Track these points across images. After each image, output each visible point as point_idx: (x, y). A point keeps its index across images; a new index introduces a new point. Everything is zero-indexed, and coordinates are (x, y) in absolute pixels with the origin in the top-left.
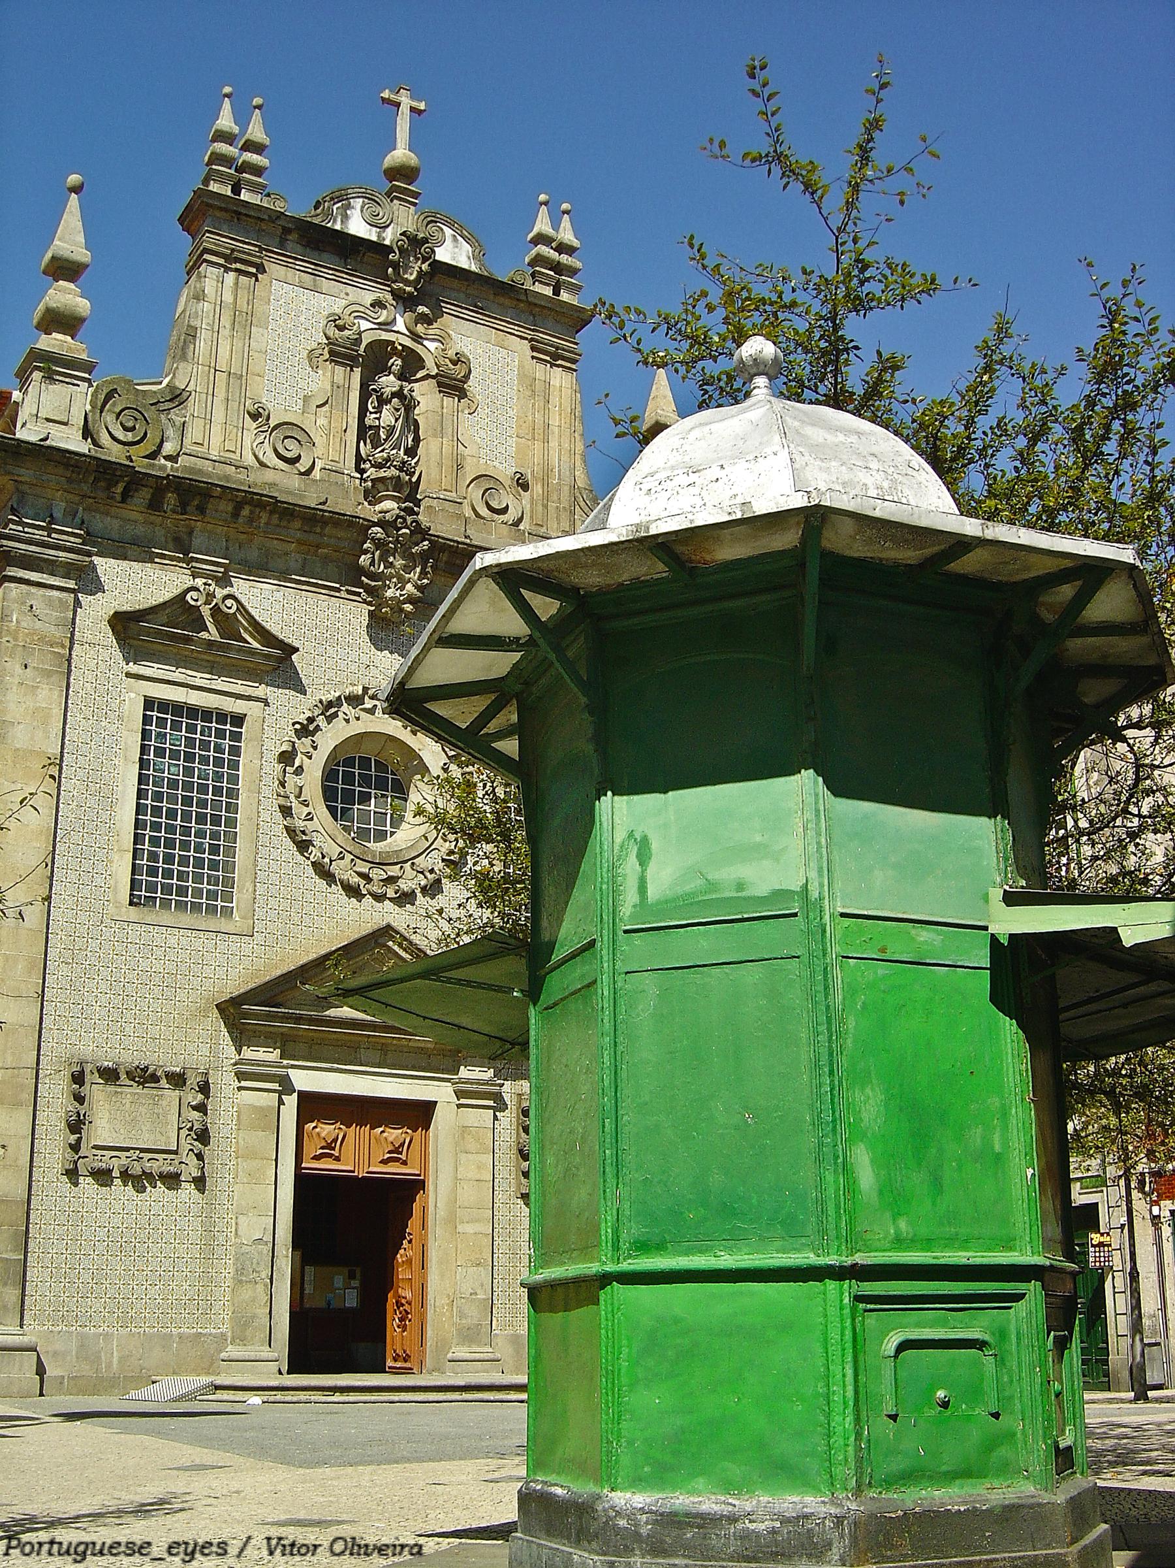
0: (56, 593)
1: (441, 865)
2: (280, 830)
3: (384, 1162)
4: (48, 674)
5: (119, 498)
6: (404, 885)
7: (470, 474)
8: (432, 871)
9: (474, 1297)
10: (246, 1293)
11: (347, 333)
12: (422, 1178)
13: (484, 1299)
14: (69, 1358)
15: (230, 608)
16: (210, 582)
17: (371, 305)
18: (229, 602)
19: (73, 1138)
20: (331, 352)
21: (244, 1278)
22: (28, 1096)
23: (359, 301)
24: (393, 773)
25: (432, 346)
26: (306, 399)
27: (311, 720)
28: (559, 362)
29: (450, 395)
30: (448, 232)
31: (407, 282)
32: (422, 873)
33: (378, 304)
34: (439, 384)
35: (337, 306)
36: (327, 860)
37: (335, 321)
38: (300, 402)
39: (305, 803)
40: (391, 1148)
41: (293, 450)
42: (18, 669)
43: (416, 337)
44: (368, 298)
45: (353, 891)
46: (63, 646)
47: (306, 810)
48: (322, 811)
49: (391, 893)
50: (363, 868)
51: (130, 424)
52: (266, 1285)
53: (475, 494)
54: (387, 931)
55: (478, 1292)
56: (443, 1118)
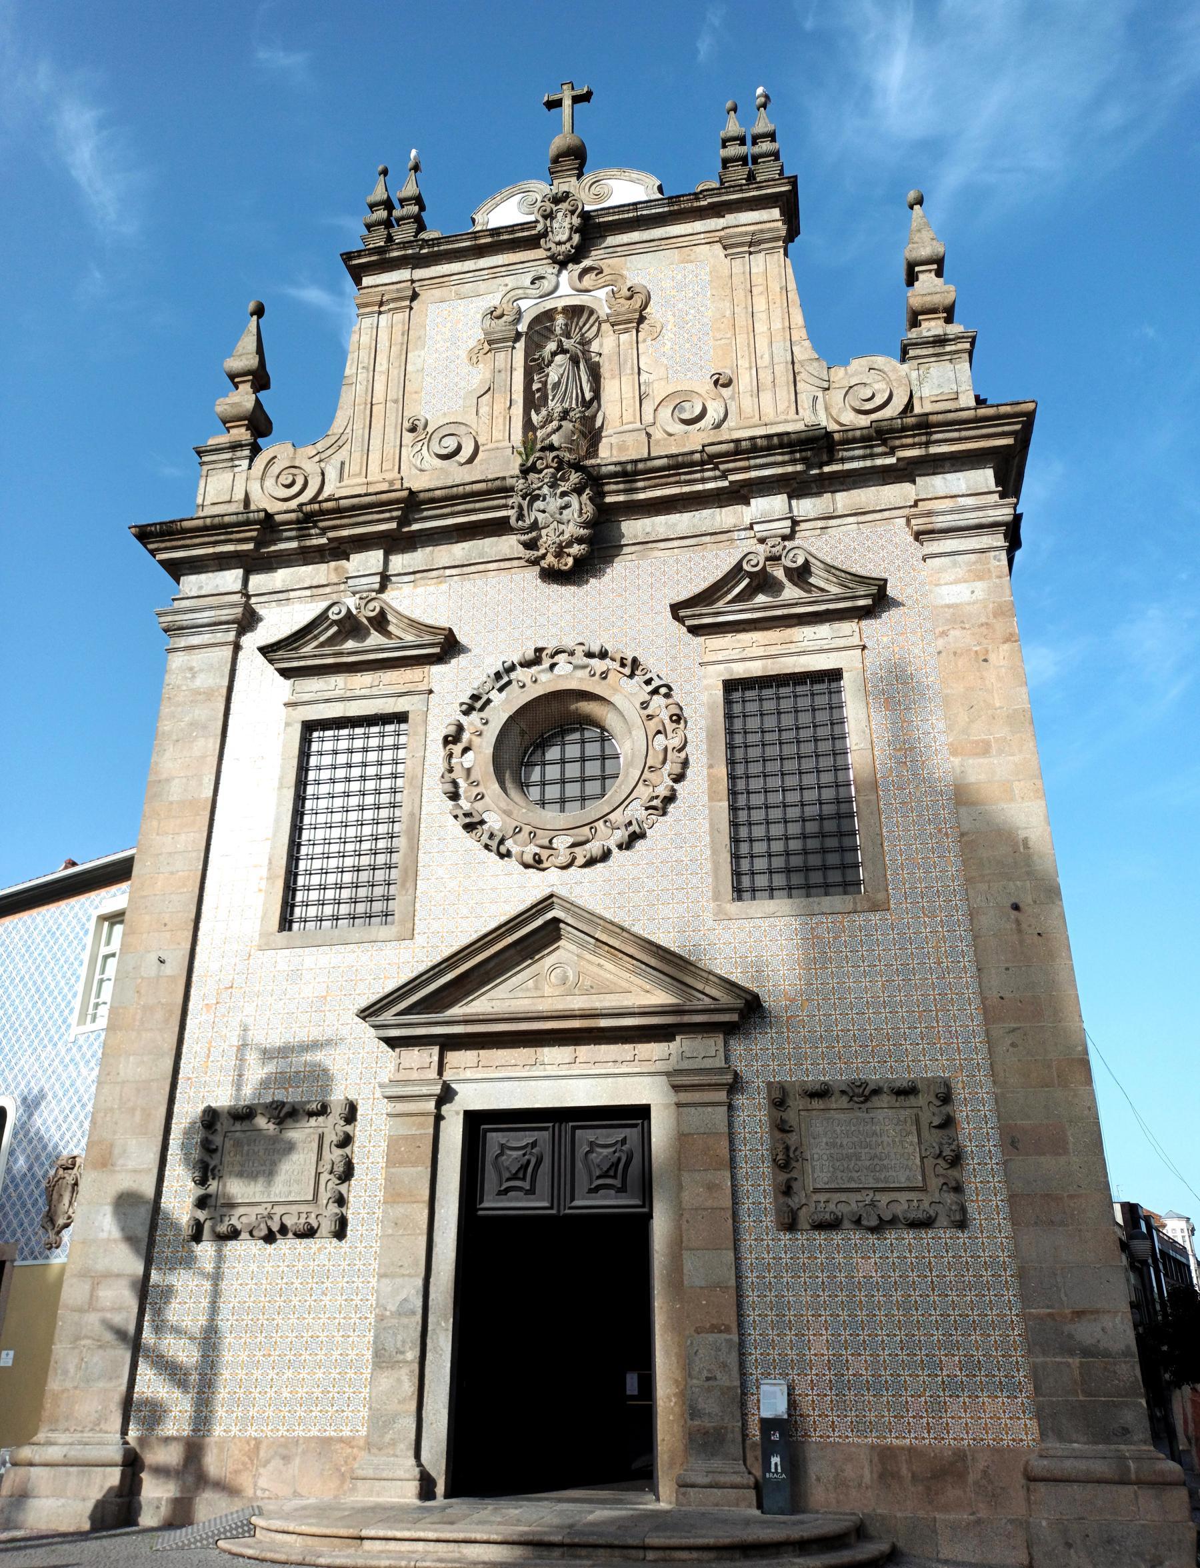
1: (645, 813)
9: (711, 1383)
17: (533, 283)
20: (490, 343)
23: (520, 285)
25: (602, 294)
28: (763, 246)
35: (494, 300)
37: (492, 312)
41: (451, 444)
51: (288, 482)
55: (719, 1376)
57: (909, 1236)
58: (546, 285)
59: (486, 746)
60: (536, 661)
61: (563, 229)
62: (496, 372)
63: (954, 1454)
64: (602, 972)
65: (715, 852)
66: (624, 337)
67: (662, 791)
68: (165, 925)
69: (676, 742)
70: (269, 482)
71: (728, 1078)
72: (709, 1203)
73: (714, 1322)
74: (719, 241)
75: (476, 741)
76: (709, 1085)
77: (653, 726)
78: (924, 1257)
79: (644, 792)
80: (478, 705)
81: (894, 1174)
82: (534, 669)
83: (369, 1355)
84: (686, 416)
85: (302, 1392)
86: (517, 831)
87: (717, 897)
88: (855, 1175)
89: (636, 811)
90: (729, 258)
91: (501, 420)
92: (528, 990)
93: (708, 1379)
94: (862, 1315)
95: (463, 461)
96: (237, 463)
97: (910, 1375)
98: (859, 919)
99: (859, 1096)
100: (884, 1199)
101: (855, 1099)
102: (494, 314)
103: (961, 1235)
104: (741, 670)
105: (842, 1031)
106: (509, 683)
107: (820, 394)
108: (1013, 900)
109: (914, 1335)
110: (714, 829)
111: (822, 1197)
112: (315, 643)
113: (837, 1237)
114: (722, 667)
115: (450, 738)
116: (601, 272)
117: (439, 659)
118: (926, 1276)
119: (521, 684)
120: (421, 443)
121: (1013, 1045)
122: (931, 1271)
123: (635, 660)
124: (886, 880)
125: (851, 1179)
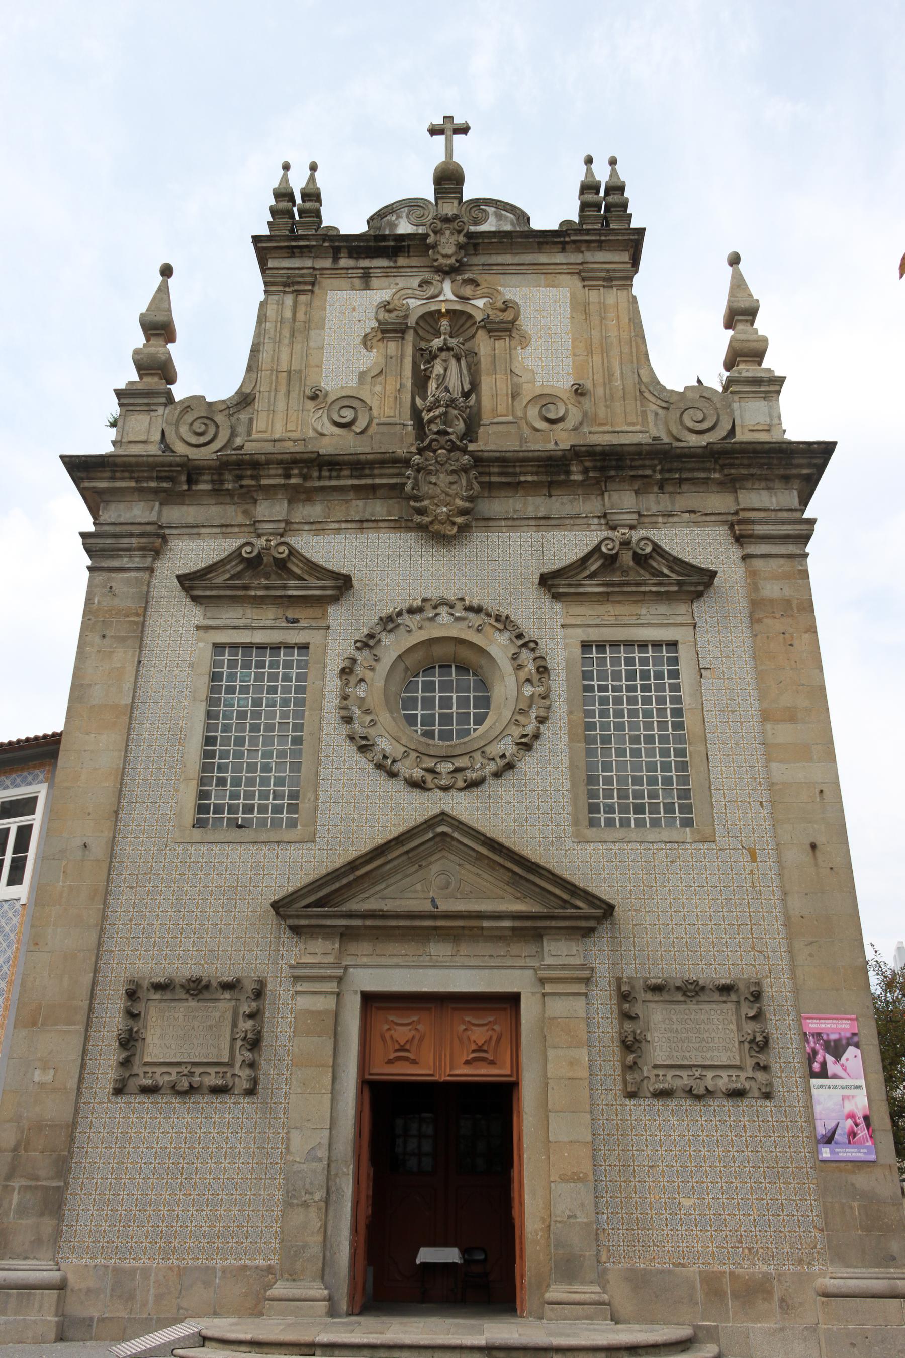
0: (133, 574)
2: (342, 739)
3: (467, 1062)
4: (123, 639)
5: (185, 487)
6: (471, 775)
7: (526, 395)
8: (503, 756)
9: (572, 1220)
10: (297, 1217)
11: (395, 313)
12: (513, 1079)
13: (586, 1224)
14: (102, 1296)
15: (281, 553)
16: (271, 538)
17: (420, 286)
18: (281, 549)
19: (124, 1055)
20: (383, 332)
21: (295, 1201)
22: (82, 1017)
23: (409, 285)
24: (474, 675)
25: (480, 303)
26: (362, 375)
27: (371, 636)
28: (614, 283)
29: (499, 338)
30: (491, 210)
31: (447, 256)
32: (493, 759)
33: (424, 283)
34: (489, 331)
36: (389, 761)
37: (385, 306)
38: (356, 379)
39: (367, 712)
40: (474, 1047)
41: (348, 415)
42: (97, 640)
43: (464, 299)
44: (415, 282)
45: (417, 785)
46: (137, 615)
47: (368, 718)
48: (384, 717)
49: (460, 784)
50: (430, 763)
52: (319, 1209)
53: (533, 413)
54: (443, 817)
55: (579, 1214)
56: (529, 1010)
57: (728, 1104)
58: (431, 291)
59: (378, 678)
60: (420, 610)
61: (448, 245)
62: (388, 358)
63: (763, 1276)
64: (480, 880)
65: (574, 785)
66: (498, 344)
67: (530, 729)
68: (89, 814)
69: (540, 690)
70: (184, 429)
71: (586, 974)
72: (570, 1074)
73: (575, 1170)
74: (579, 273)
75: (368, 675)
76: (572, 978)
77: (523, 675)
78: (740, 1121)
79: (516, 732)
80: (371, 643)
81: (718, 1054)
82: (418, 617)
83: (279, 1195)
84: (552, 416)
85: (219, 1226)
86: (406, 755)
87: (576, 822)
88: (687, 1054)
89: (507, 746)
90: (586, 289)
91: (392, 400)
92: (416, 891)
93: (569, 1217)
94: (691, 1166)
95: (359, 430)
96: (153, 408)
97: (729, 1215)
98: (691, 848)
99: (691, 991)
100: (710, 1074)
101: (689, 994)
102: (386, 307)
103: (769, 1104)
104: (594, 635)
105: (677, 938)
106: (398, 626)
107: (660, 411)
108: (812, 840)
109: (732, 1183)
110: (572, 767)
111: (661, 1072)
112: (228, 576)
113: (672, 1104)
114: (579, 631)
115: (347, 670)
116: (478, 285)
117: (335, 599)
118: (741, 1136)
119: (408, 629)
120: (321, 411)
121: (811, 955)
122: (745, 1131)
123: (507, 617)
124: (713, 817)
125: (684, 1058)
